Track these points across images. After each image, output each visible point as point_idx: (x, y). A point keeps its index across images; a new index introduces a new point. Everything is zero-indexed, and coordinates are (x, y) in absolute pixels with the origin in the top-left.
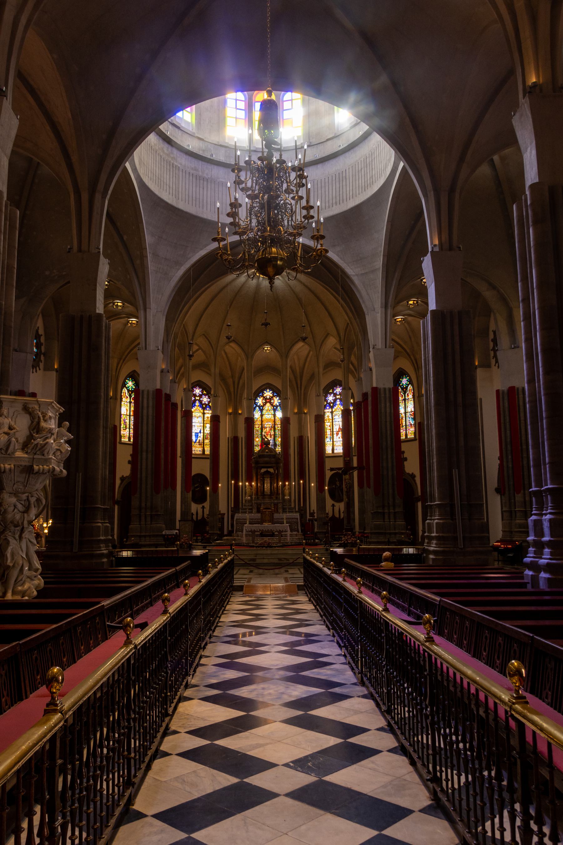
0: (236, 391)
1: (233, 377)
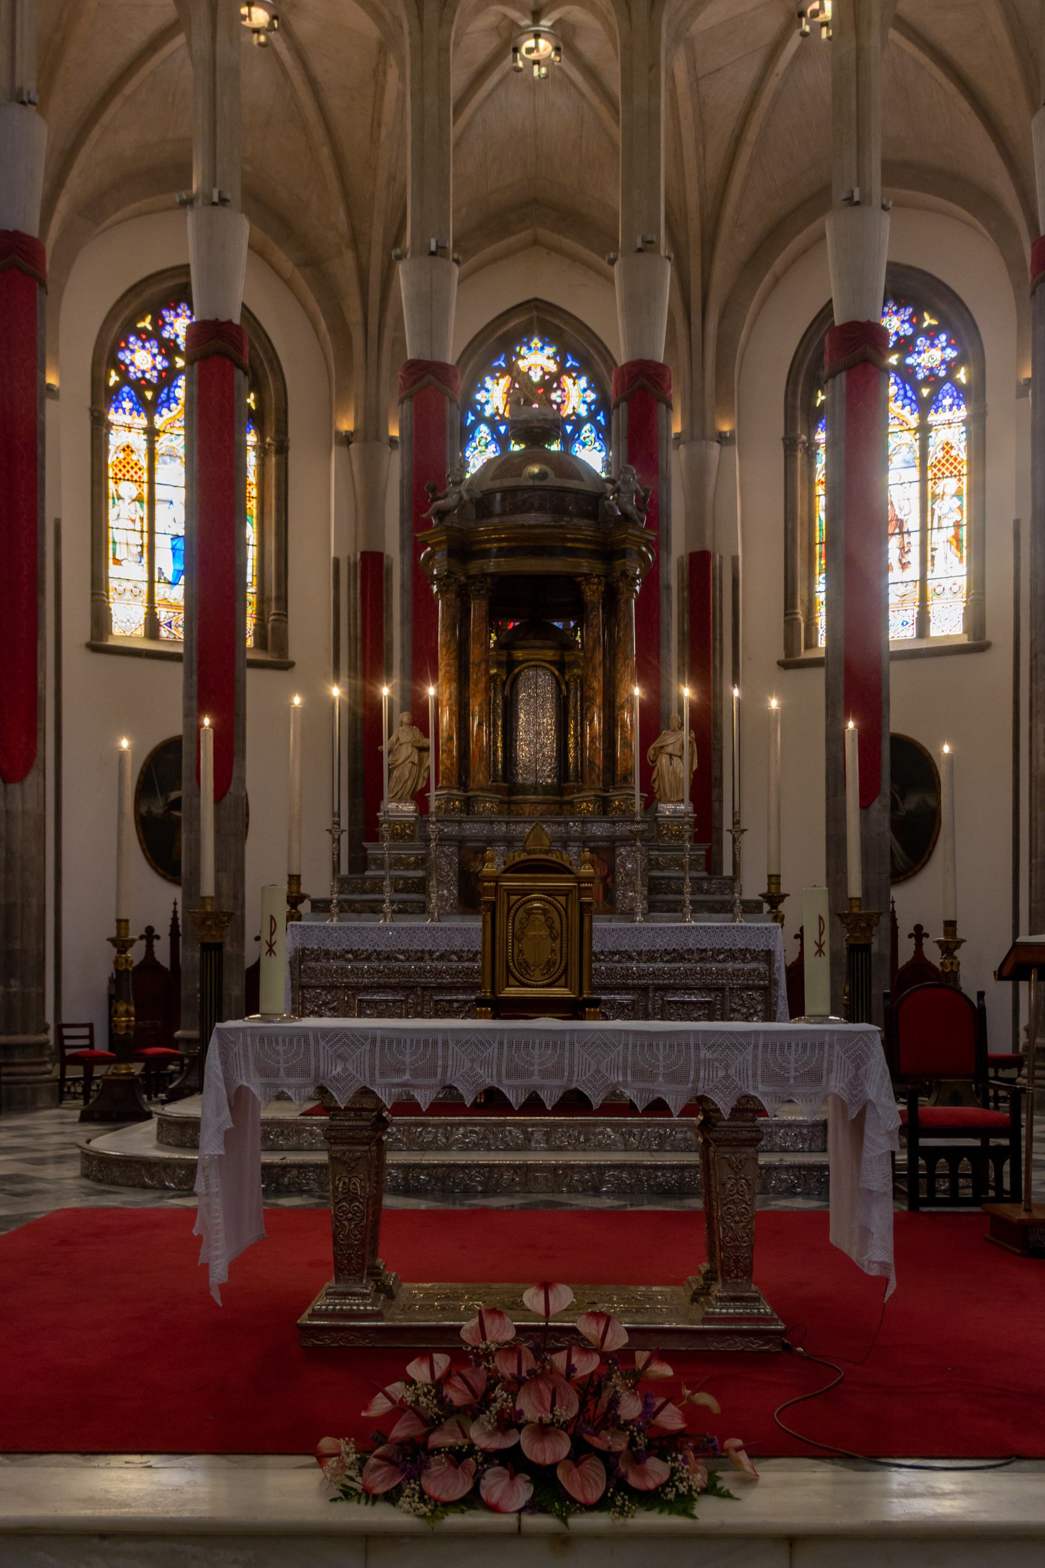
0: (373, 319)
1: (356, 240)
